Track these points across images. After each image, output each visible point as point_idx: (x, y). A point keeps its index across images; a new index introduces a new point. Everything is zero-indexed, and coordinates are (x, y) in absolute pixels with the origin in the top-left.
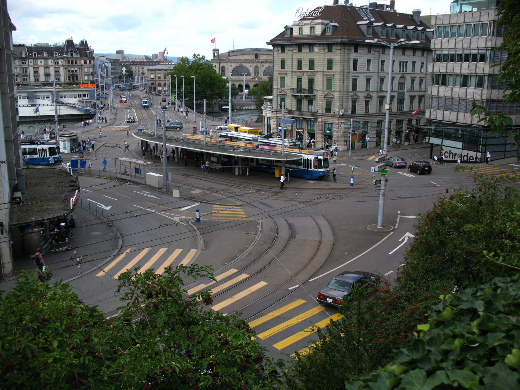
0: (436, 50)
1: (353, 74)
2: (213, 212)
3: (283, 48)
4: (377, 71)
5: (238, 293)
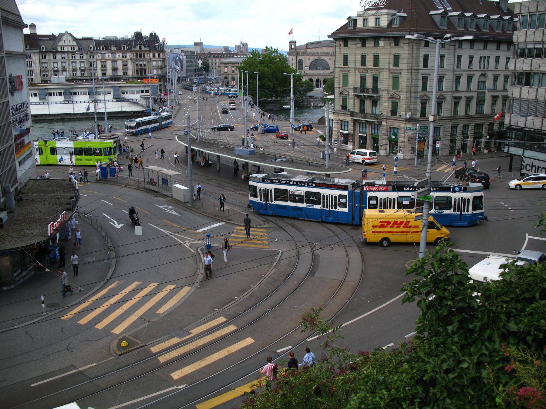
0: (519, 43)
1: (423, 71)
3: (346, 41)
4: (452, 69)
5: (212, 353)
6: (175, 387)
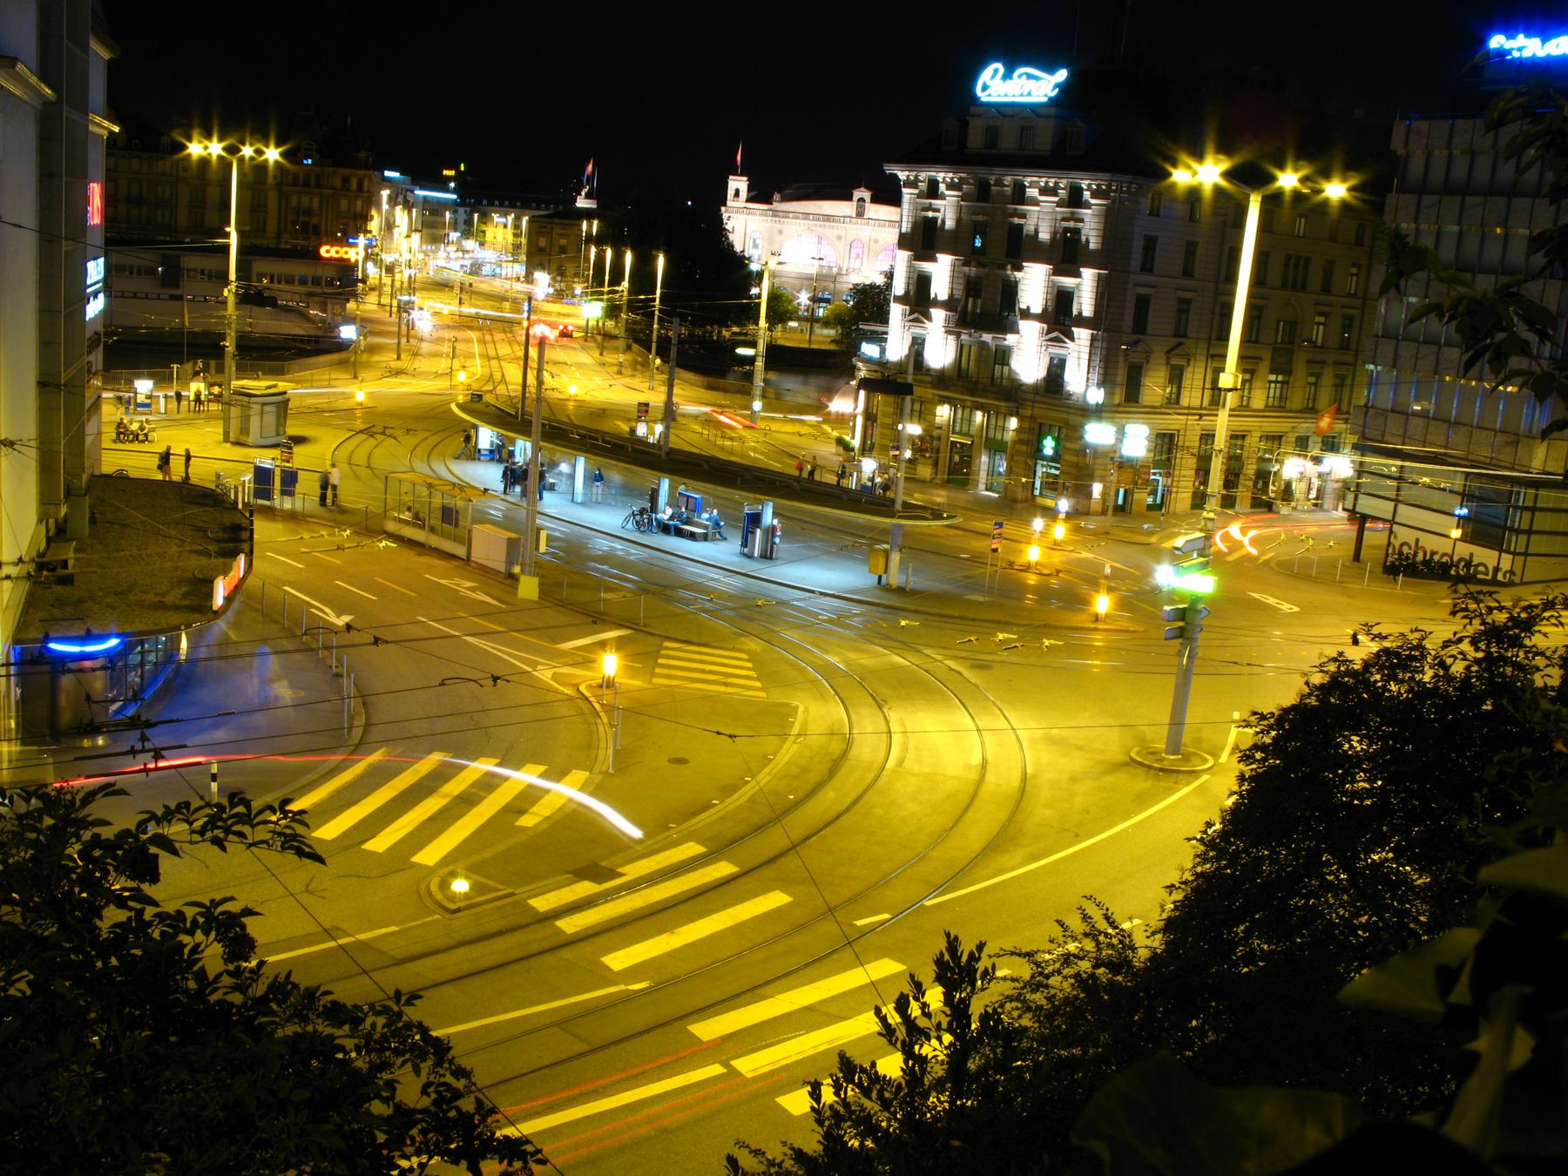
2: (661, 661)
5: (692, 920)
6: (623, 987)
